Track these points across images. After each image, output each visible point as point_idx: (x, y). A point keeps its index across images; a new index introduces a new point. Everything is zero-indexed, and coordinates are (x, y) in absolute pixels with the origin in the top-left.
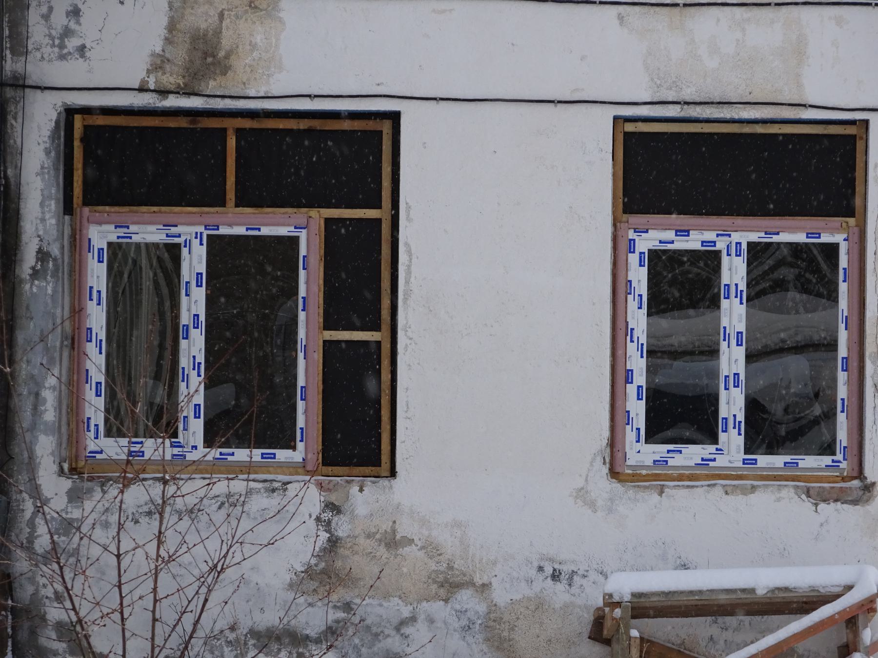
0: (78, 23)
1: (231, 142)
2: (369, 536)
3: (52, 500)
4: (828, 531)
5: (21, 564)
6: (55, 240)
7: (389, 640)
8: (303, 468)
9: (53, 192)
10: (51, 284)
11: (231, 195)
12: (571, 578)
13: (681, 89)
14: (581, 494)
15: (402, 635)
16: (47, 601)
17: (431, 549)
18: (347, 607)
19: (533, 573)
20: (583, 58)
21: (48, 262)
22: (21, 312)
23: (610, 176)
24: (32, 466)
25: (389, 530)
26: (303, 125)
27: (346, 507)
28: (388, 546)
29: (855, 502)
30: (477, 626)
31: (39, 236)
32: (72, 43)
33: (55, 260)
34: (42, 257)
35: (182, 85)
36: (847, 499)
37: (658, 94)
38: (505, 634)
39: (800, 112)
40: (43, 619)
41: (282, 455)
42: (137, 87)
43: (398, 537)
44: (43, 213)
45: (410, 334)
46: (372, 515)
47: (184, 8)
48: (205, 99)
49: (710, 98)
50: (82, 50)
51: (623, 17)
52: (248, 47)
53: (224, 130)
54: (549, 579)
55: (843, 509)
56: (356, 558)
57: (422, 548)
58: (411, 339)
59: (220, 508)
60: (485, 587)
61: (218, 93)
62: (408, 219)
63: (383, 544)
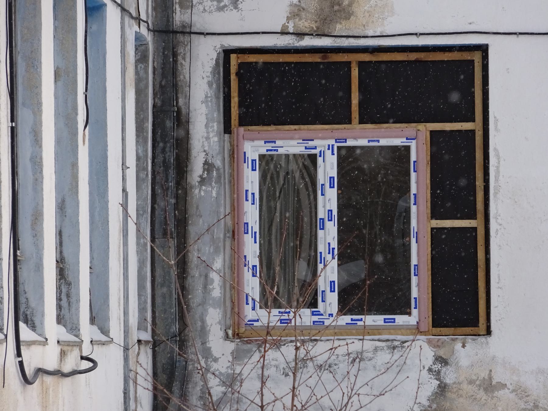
1: (355, 73)
2: (471, 382)
3: (220, 359)
6: (218, 154)
8: (417, 330)
9: (215, 115)
10: (215, 189)
11: (355, 115)
21: (213, 171)
22: (192, 210)
24: (204, 332)
25: (486, 378)
26: (413, 56)
28: (486, 390)
31: (205, 151)
33: (218, 170)
34: (208, 168)
35: (315, 29)
41: (400, 319)
43: (494, 383)
44: (208, 133)
45: (499, 221)
46: (472, 365)
48: (333, 38)
53: (349, 63)
56: (461, 400)
57: (513, 391)
61: (344, 34)
62: (496, 129)
63: (482, 388)
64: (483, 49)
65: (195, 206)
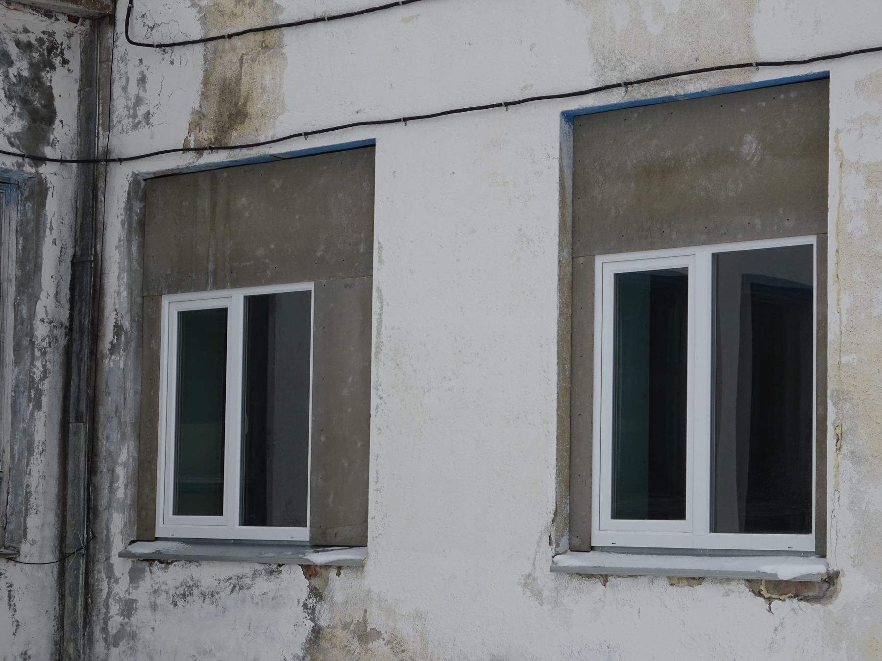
0: (145, 90)
2: (345, 627)
3: (120, 580)
4: (784, 638)
6: (127, 313)
9: (126, 264)
10: (123, 358)
13: (625, 67)
14: (528, 582)
21: (121, 336)
22: (102, 387)
23: (557, 186)
24: (108, 543)
27: (325, 594)
28: (360, 638)
29: (817, 599)
31: (116, 310)
32: (141, 111)
33: (126, 333)
34: (118, 331)
35: (213, 140)
36: (806, 594)
37: (602, 78)
39: (750, 75)
42: (182, 148)
43: (368, 629)
44: (119, 286)
45: (380, 393)
46: (347, 602)
47: (215, 59)
48: (228, 151)
49: (655, 74)
50: (147, 115)
52: (260, 91)
55: (801, 609)
56: (335, 651)
57: (389, 642)
58: (381, 398)
59: (232, 592)
61: (238, 144)
62: (381, 261)
63: (357, 636)
64: (370, 145)
65: (105, 381)
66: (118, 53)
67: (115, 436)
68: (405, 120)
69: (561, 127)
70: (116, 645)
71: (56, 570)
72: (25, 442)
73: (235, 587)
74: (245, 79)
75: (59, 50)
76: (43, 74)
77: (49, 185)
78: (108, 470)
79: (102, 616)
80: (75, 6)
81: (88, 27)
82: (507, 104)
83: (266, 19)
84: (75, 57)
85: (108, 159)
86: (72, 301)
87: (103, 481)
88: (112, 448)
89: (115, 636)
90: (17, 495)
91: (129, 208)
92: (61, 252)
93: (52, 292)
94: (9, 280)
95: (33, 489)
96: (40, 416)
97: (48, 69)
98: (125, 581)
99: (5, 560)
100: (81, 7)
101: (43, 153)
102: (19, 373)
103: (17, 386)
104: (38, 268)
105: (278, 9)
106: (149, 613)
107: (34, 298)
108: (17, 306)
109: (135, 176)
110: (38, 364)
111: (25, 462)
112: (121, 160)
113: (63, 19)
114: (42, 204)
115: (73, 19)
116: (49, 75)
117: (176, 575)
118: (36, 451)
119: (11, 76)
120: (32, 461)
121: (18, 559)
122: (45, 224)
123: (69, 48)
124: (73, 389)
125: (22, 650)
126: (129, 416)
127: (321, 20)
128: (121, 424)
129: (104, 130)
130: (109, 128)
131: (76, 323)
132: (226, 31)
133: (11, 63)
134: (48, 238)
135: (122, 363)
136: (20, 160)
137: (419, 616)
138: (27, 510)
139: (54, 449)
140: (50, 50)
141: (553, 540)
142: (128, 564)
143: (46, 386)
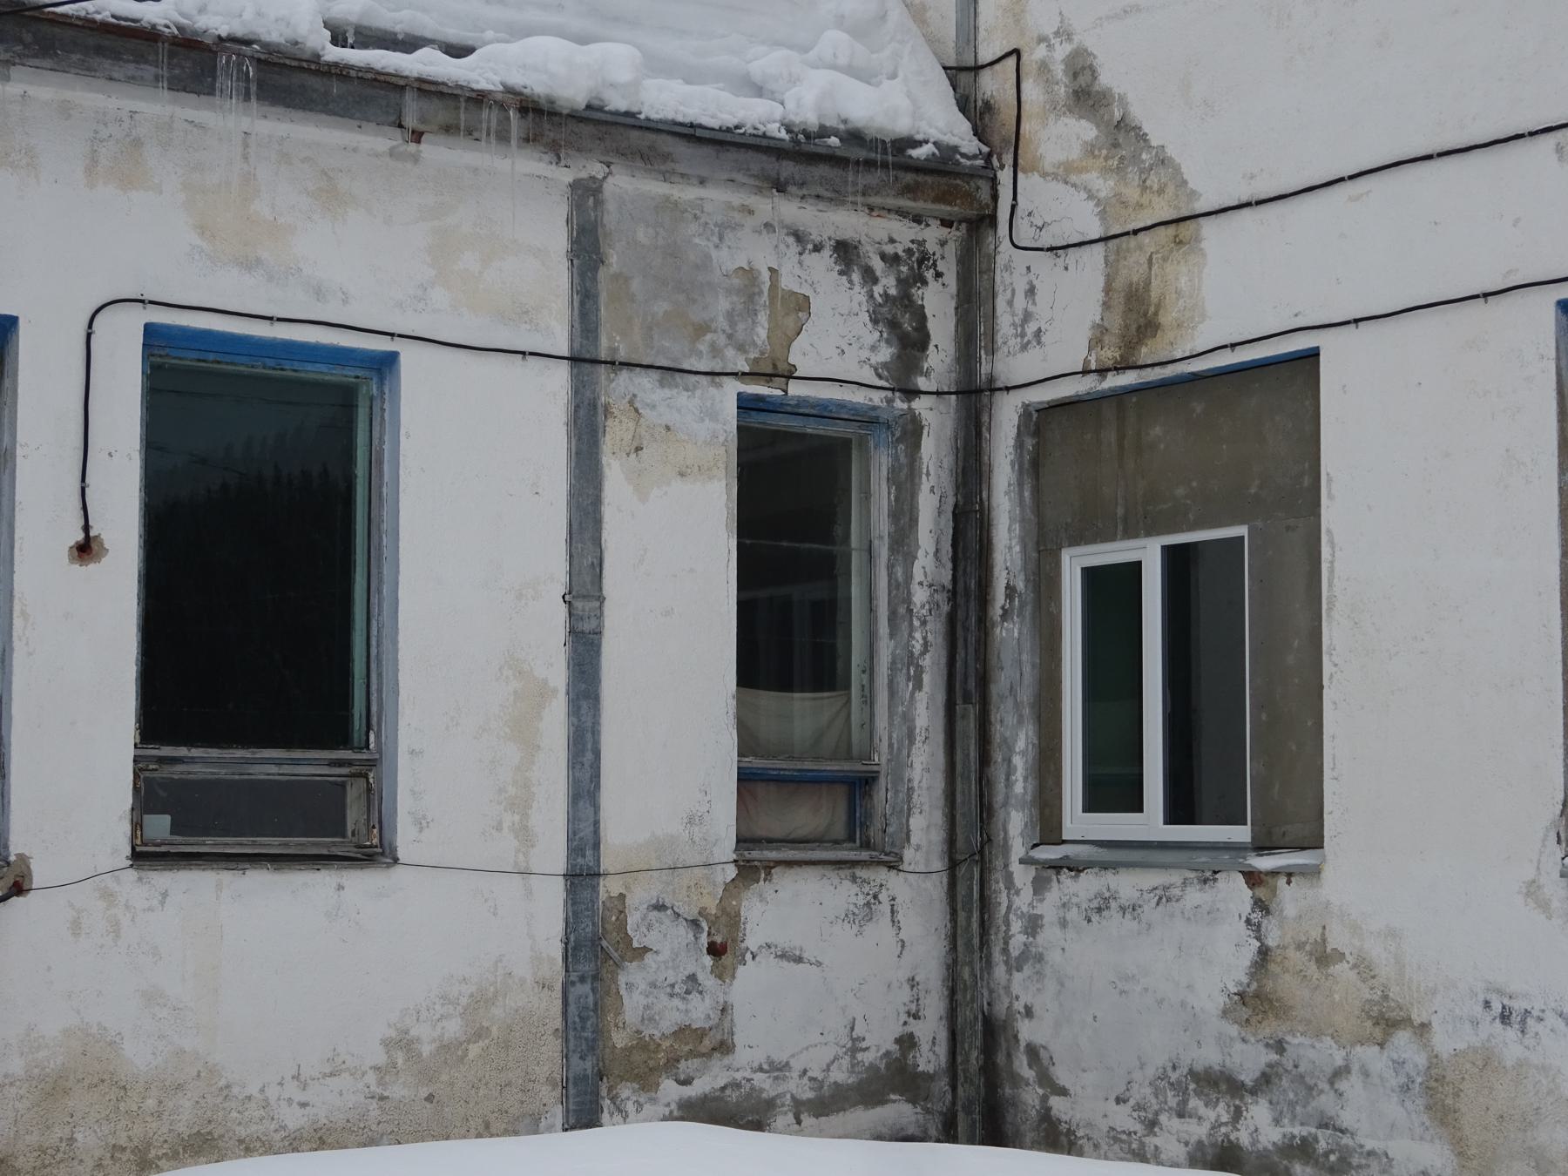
0: (1034, 303)
2: (1300, 946)
5: (1000, 971)
7: (1323, 1097)
12: (1523, 1022)
14: (1532, 890)
15: (1336, 1091)
16: (1018, 1016)
17: (1365, 968)
18: (1279, 1046)
19: (1478, 1009)
20: (1516, 222)
22: (993, 661)
23: (1554, 394)
24: (1006, 849)
25: (1319, 940)
27: (1273, 907)
30: (1417, 1085)
32: (1031, 328)
38: (1449, 1101)
40: (1016, 1037)
42: (1081, 370)
43: (1328, 950)
45: (1334, 658)
46: (1300, 916)
47: (1118, 261)
51: (1562, 148)
52: (1174, 296)
54: (1498, 1020)
56: (1287, 977)
57: (1355, 966)
58: (1336, 665)
59: (1158, 904)
60: (1425, 1027)
61: (1149, 362)
62: (1330, 496)
64: (1313, 355)
66: (1001, 260)
67: (1011, 719)
68: (1357, 321)
69: (1557, 320)
70: (1019, 969)
71: (945, 880)
72: (905, 728)
73: (1160, 898)
74: (1154, 283)
75: (931, 262)
76: (913, 291)
77: (924, 423)
78: (1004, 760)
79: (1001, 935)
80: (949, 208)
81: (964, 231)
82: (1486, 295)
83: (1180, 208)
84: (949, 268)
85: (992, 388)
86: (955, 560)
87: (998, 772)
88: (1008, 734)
89: (1017, 959)
90: (896, 792)
91: (1019, 444)
92: (940, 501)
93: (932, 550)
94: (881, 538)
95: (915, 784)
96: (922, 698)
97: (919, 285)
98: (1027, 894)
99: (886, 869)
100: (956, 209)
101: (917, 385)
102: (896, 647)
103: (893, 662)
104: (914, 521)
105: (1193, 195)
106: (1057, 930)
107: (910, 558)
108: (890, 567)
109: (1026, 406)
110: (918, 635)
111: (905, 752)
112: (1008, 389)
113: (935, 223)
114: (917, 446)
115: (946, 223)
116: (920, 292)
117: (1087, 885)
118: (918, 738)
119: (876, 295)
120: (914, 751)
121: (901, 868)
122: (920, 469)
123: (943, 258)
124: (959, 665)
125: (909, 975)
126: (1026, 695)
127: (1248, 205)
128: (1017, 705)
129: (986, 354)
130: (992, 351)
131: (961, 585)
132: (1130, 227)
133: (875, 281)
134: (925, 486)
135: (1016, 631)
136: (889, 394)
137: (1392, 933)
138: (909, 809)
139: (939, 737)
140: (921, 262)
141: (1563, 838)
142: (1031, 872)
143: (927, 662)
